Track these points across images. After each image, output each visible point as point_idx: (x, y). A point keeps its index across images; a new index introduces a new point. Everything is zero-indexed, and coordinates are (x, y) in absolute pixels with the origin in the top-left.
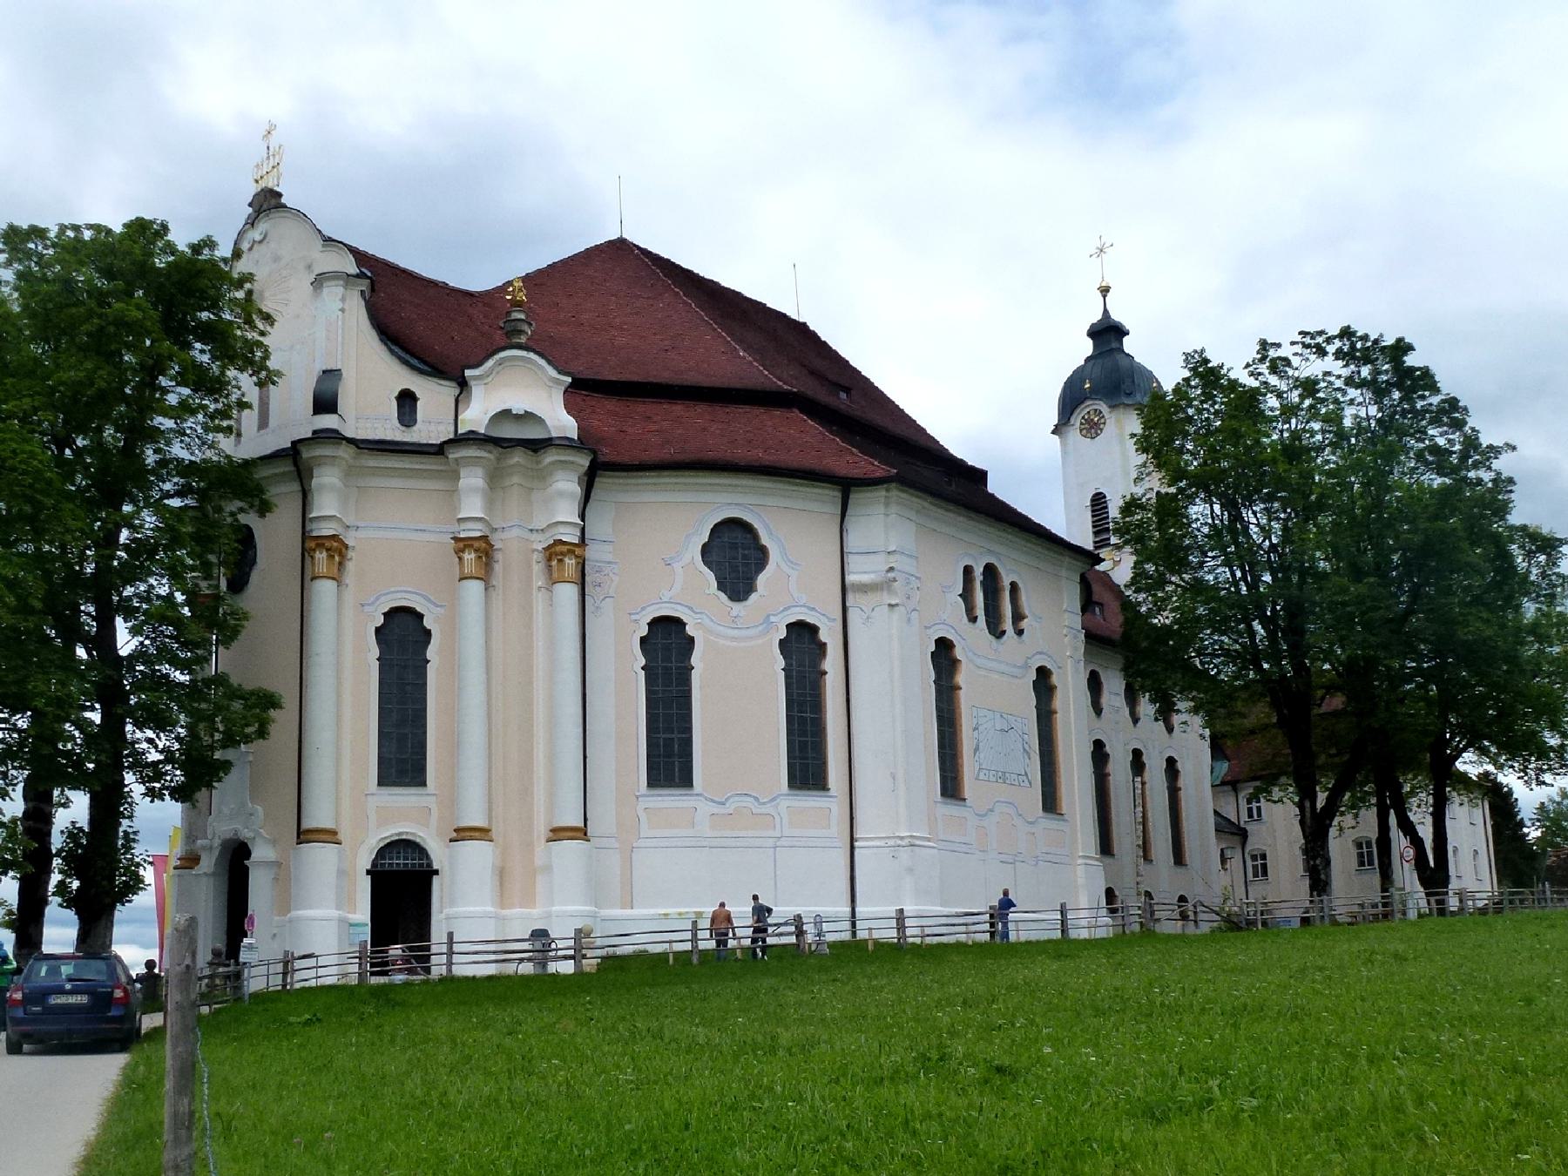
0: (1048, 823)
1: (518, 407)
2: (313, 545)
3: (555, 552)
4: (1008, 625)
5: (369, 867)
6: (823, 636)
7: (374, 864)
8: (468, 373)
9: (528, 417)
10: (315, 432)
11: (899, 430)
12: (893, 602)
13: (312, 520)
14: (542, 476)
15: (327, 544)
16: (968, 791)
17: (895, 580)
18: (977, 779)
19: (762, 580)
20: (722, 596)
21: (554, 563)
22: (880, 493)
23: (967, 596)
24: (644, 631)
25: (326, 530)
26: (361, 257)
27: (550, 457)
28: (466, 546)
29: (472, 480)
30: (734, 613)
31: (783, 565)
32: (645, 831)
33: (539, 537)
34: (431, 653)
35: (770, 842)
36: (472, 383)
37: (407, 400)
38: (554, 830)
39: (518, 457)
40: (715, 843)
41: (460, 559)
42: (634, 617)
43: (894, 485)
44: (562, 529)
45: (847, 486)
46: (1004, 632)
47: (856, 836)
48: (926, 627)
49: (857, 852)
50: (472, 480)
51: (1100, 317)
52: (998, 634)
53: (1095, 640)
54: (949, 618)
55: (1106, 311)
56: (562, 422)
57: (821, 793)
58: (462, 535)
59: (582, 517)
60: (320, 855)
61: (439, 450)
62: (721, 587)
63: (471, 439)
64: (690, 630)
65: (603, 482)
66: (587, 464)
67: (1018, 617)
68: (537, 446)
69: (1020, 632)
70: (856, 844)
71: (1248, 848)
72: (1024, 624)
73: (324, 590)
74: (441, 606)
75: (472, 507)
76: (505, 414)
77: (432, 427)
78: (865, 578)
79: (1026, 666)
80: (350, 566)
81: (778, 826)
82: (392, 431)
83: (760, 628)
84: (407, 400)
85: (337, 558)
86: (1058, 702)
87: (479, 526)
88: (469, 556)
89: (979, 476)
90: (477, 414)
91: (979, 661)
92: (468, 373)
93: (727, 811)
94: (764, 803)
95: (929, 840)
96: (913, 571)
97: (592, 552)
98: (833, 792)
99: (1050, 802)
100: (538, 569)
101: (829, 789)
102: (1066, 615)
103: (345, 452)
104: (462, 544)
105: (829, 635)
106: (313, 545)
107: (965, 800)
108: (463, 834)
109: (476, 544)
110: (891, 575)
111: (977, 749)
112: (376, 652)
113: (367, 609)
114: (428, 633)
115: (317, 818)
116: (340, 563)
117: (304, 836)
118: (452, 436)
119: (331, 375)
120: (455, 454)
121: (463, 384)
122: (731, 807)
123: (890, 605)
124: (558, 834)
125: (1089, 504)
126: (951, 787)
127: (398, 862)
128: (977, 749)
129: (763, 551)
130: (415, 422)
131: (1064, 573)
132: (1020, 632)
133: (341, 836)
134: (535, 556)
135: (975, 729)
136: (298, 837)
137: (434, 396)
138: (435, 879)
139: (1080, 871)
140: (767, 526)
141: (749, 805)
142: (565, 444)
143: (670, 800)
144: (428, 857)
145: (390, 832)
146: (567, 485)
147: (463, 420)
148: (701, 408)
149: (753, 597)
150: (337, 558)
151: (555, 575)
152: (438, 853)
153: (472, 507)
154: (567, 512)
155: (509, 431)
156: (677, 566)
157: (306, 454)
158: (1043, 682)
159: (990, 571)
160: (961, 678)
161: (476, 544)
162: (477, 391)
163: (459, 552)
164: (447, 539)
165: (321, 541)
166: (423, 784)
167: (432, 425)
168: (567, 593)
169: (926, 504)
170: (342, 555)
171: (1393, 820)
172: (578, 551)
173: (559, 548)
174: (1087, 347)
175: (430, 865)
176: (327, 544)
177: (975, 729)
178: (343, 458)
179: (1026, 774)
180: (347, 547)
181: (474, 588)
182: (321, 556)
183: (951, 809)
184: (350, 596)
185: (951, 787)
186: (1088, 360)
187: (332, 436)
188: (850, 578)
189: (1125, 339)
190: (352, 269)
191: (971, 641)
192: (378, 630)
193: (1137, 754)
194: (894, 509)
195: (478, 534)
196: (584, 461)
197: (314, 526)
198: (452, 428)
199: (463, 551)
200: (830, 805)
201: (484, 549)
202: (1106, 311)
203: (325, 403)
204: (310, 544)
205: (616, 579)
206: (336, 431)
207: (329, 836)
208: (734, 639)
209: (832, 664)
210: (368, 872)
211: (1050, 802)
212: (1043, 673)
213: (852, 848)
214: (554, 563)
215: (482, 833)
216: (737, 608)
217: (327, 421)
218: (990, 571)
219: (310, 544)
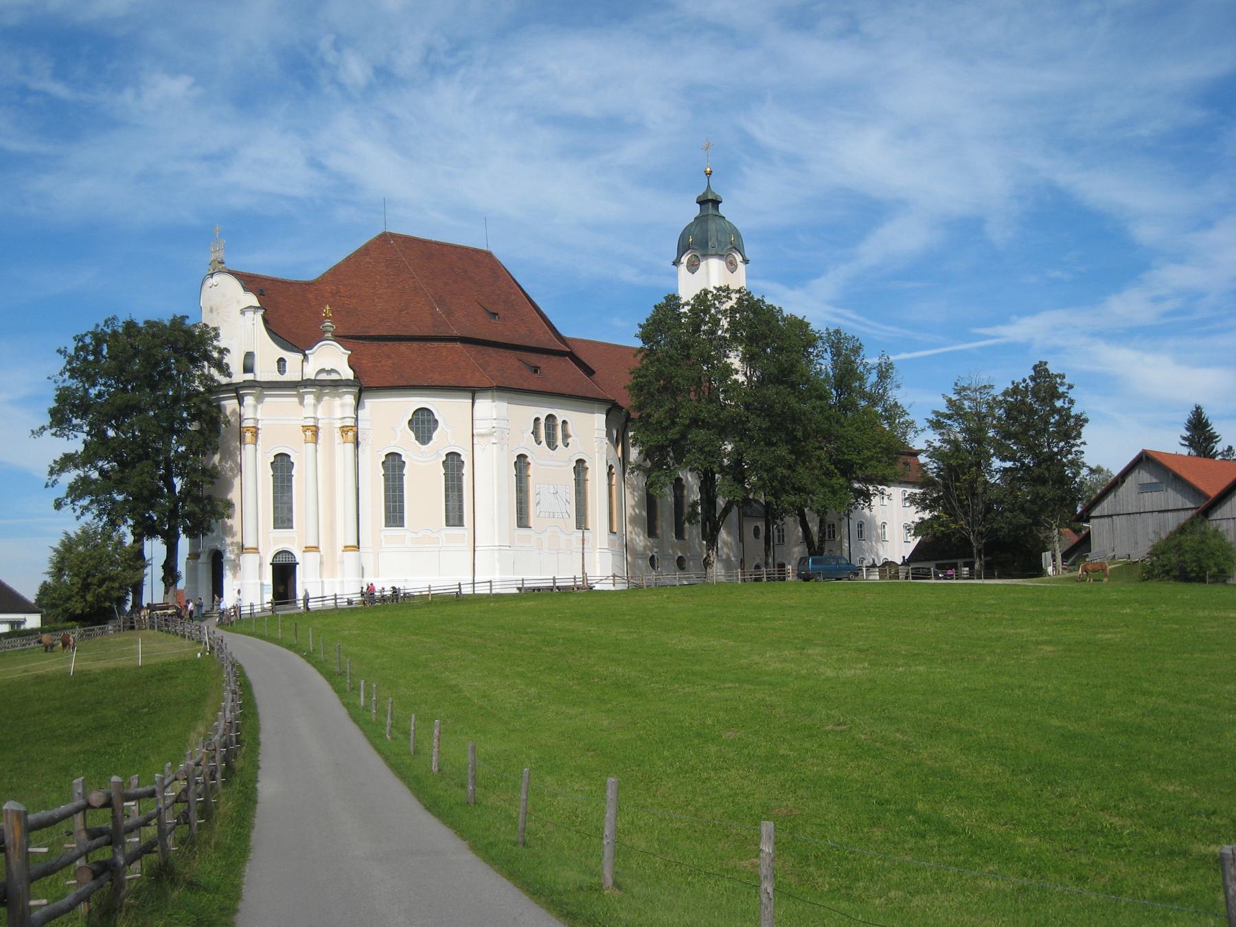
3: (344, 430)
4: (559, 442)
5: (271, 562)
6: (463, 458)
7: (273, 561)
8: (307, 352)
9: (333, 371)
12: (494, 442)
16: (532, 523)
17: (495, 432)
19: (435, 435)
20: (417, 442)
22: (490, 393)
23: (535, 433)
29: (309, 399)
30: (422, 450)
31: (444, 427)
36: (309, 356)
37: (281, 362)
38: (345, 547)
46: (557, 446)
47: (476, 545)
49: (476, 553)
50: (309, 399)
51: (704, 190)
54: (526, 444)
55: (709, 186)
56: (349, 374)
66: (357, 391)
67: (566, 436)
68: (337, 385)
69: (567, 445)
70: (476, 549)
72: (570, 440)
75: (308, 411)
76: (322, 371)
78: (483, 431)
79: (570, 460)
82: (276, 377)
84: (281, 362)
88: (309, 433)
90: (310, 372)
100: (338, 434)
101: (463, 526)
108: (308, 549)
110: (494, 430)
112: (272, 473)
113: (267, 454)
121: (305, 356)
123: (493, 443)
124: (347, 549)
126: (522, 520)
127: (282, 560)
129: (436, 421)
132: (567, 445)
137: (293, 358)
138: (297, 566)
140: (438, 412)
145: (280, 547)
146: (350, 400)
149: (431, 442)
154: (350, 412)
155: (323, 376)
159: (551, 418)
163: (304, 431)
166: (292, 528)
167: (292, 375)
168: (350, 446)
173: (345, 429)
174: (696, 211)
177: (537, 494)
180: (259, 429)
181: (311, 446)
185: (522, 520)
186: (696, 218)
191: (538, 455)
196: (356, 390)
200: (464, 532)
202: (709, 186)
203: (248, 369)
205: (372, 436)
208: (422, 462)
209: (466, 470)
210: (271, 564)
212: (580, 462)
216: (424, 447)
218: (551, 418)
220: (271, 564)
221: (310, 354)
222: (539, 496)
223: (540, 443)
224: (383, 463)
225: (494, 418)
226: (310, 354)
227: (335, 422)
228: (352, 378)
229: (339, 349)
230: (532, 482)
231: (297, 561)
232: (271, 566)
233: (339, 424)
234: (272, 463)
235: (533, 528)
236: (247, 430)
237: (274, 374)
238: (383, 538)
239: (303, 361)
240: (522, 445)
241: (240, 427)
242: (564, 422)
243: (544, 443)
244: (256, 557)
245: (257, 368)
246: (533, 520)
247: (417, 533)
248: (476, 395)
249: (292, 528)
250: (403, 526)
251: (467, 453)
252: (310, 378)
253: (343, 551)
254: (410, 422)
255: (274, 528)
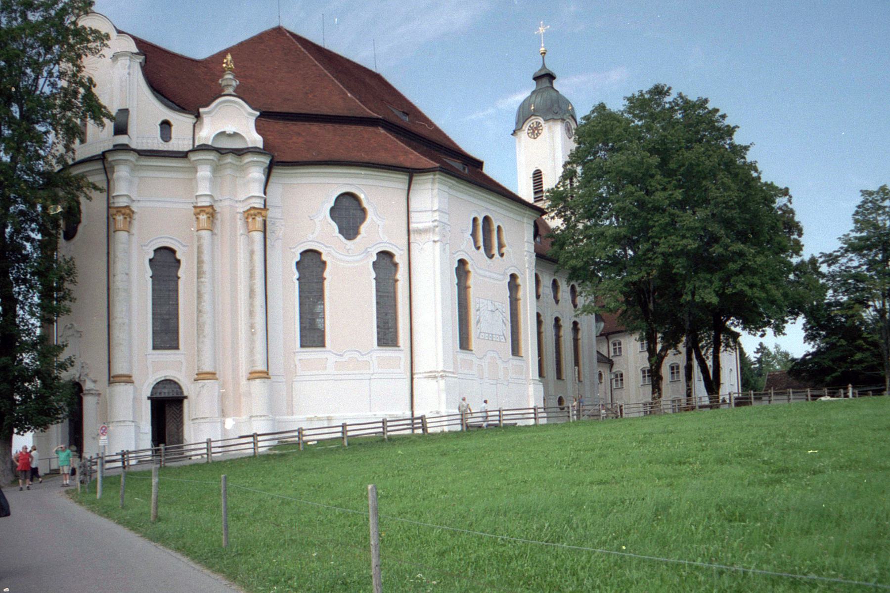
0: (515, 361)
1: (230, 129)
2: (114, 211)
3: (250, 214)
4: (495, 251)
5: (149, 395)
6: (397, 259)
7: (152, 393)
8: (201, 110)
9: (235, 135)
10: (115, 146)
11: (434, 137)
13: (113, 197)
14: (242, 169)
15: (123, 211)
18: (478, 338)
19: (363, 228)
21: (250, 220)
23: (474, 234)
24: (298, 258)
25: (121, 202)
26: (139, 42)
27: (248, 158)
28: (201, 211)
29: (204, 172)
30: (348, 247)
31: (375, 219)
32: (299, 372)
33: (240, 205)
34: (180, 273)
35: (367, 377)
36: (204, 116)
37: (166, 125)
38: (251, 373)
39: (230, 159)
40: (338, 377)
41: (197, 218)
42: (293, 250)
43: (437, 172)
44: (253, 200)
45: (411, 172)
46: (493, 255)
47: (415, 371)
48: (453, 254)
49: (415, 381)
50: (204, 172)
52: (491, 256)
53: (540, 256)
54: (467, 249)
56: (255, 139)
57: (397, 348)
58: (199, 205)
59: (265, 193)
60: (121, 390)
61: (184, 155)
62: (341, 232)
63: (204, 148)
64: (324, 258)
65: (276, 171)
66: (268, 162)
67: (501, 246)
68: (239, 153)
69: (502, 255)
71: (614, 370)
72: (504, 250)
73: (122, 236)
74: (186, 246)
76: (223, 134)
77: (180, 142)
78: (421, 226)
79: (504, 274)
80: (135, 223)
81: (372, 368)
82: (157, 144)
83: (361, 256)
84: (166, 125)
85: (128, 219)
86: (520, 294)
87: (208, 199)
88: (203, 217)
89: (479, 164)
90: (207, 133)
91: (481, 272)
92: (201, 110)
93: (343, 360)
94: (366, 355)
95: (453, 373)
96: (446, 221)
97: (270, 214)
98: (402, 348)
99: (516, 350)
100: (240, 223)
102: (526, 244)
103: (132, 157)
104: (199, 210)
105: (400, 258)
106: (114, 211)
107: (471, 350)
108: (202, 376)
109: (207, 210)
111: (478, 322)
112: (150, 273)
114: (179, 261)
115: (120, 368)
116: (130, 222)
117: (113, 379)
118: (191, 148)
119: (125, 112)
120: (193, 157)
121: (198, 116)
122: (346, 357)
123: (434, 241)
124: (254, 375)
125: (531, 176)
126: (464, 343)
127: (166, 393)
128: (478, 322)
129: (364, 211)
130: (170, 138)
131: (525, 220)
132: (502, 255)
133: (133, 379)
134: (239, 216)
135: (477, 310)
136: (109, 380)
137: (181, 122)
138: (186, 402)
139: (531, 389)
141: (355, 356)
142: (254, 151)
143: (313, 354)
144: (180, 388)
145: (161, 376)
146: (257, 174)
147: (199, 138)
148: (329, 127)
149: (359, 237)
150: (128, 219)
151: (251, 227)
152: (188, 388)
153: (204, 188)
156: (317, 220)
157: (110, 158)
158: (513, 283)
159: (487, 219)
160: (471, 282)
161: (207, 210)
162: (206, 120)
163: (196, 214)
164: (191, 206)
165: (119, 210)
166: (177, 348)
167: (180, 141)
168: (258, 236)
169: (454, 182)
170: (130, 217)
171: (694, 356)
172: (263, 213)
173: (252, 212)
175: (182, 392)
176: (123, 211)
177: (477, 310)
178: (131, 161)
179: (504, 335)
180: (133, 212)
181: (205, 234)
182: (120, 218)
183: (463, 355)
184: (135, 239)
187: (124, 148)
188: (412, 226)
189: (554, 81)
190: (135, 50)
191: (476, 260)
192: (151, 260)
193: (557, 320)
194: (437, 186)
195: (208, 204)
196: (266, 160)
197: (116, 200)
198: (191, 142)
199: (199, 214)
200: (400, 355)
201: (211, 213)
203: (121, 129)
204: (112, 211)
206: (127, 145)
207: (128, 379)
209: (401, 275)
210: (149, 398)
211: (516, 350)
212: (513, 277)
213: (412, 379)
214: (250, 220)
215: (212, 375)
217: (122, 139)
218: (487, 219)
219: (112, 211)
220: (149, 398)
221: (206, 113)
222: (478, 313)
223: (478, 248)
224: (297, 263)
225: (435, 209)
226: (206, 113)
227: (237, 205)
228: (261, 146)
229: (246, 110)
230: (472, 293)
231: (185, 394)
232: (149, 402)
233: (242, 208)
234: (151, 260)
235: (474, 352)
236: (118, 212)
237: (155, 141)
238: (297, 363)
239: (194, 126)
240: (462, 248)
241: (109, 207)
242: (499, 227)
243: (482, 248)
244: (129, 387)
245: (132, 128)
246: (474, 342)
247: (341, 355)
248: (415, 178)
249: (177, 348)
250: (323, 346)
251: (401, 252)
252: (206, 143)
253: (249, 379)
254: (332, 210)
255: (154, 348)
